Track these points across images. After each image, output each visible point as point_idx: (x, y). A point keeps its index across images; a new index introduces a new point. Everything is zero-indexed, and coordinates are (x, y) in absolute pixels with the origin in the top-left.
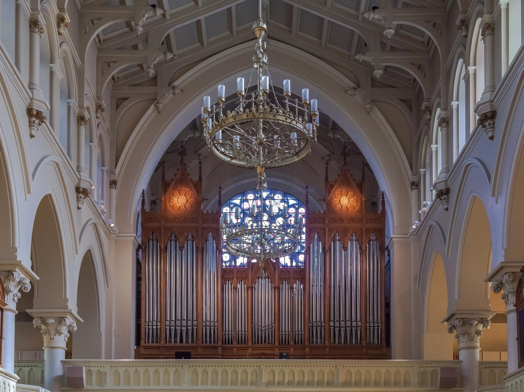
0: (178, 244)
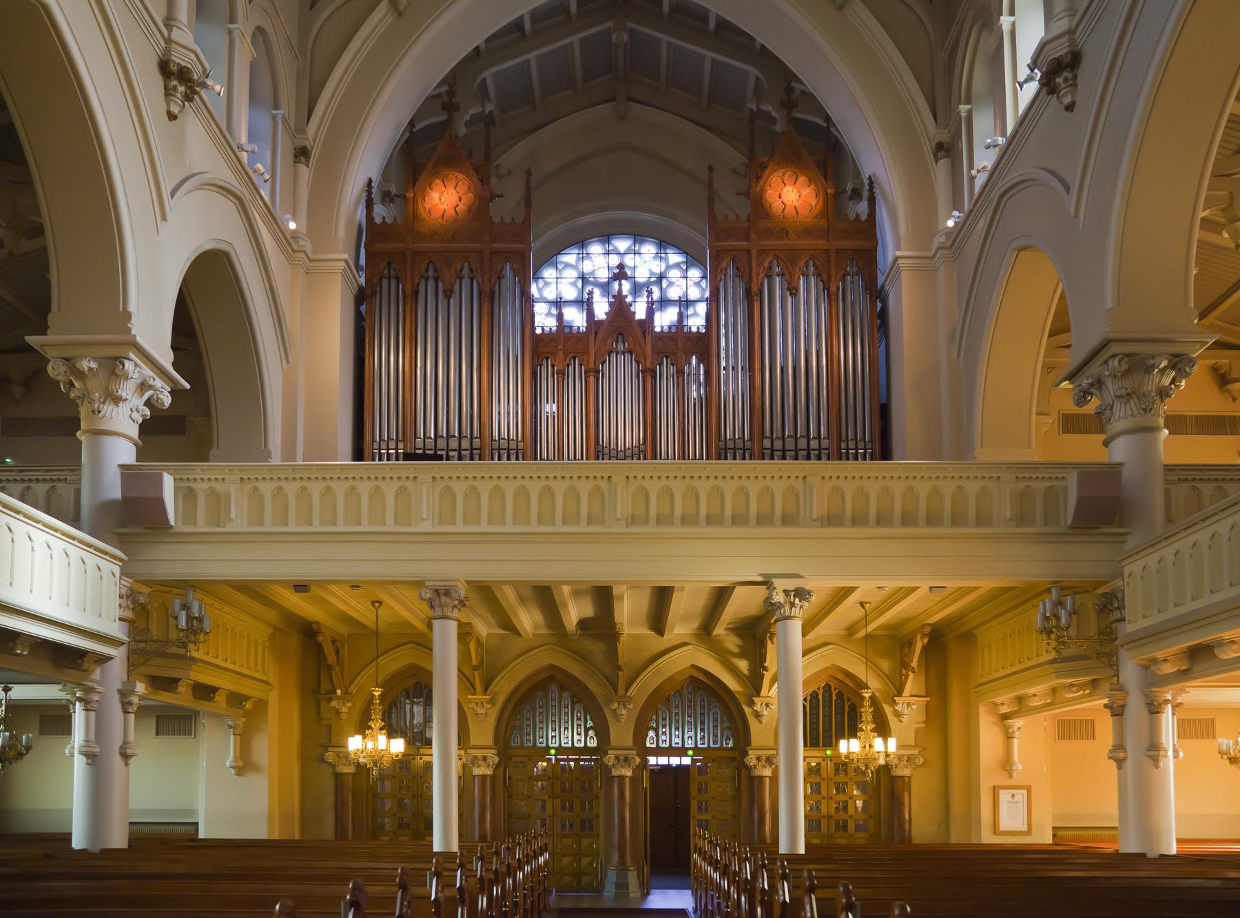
0: (440, 285)
